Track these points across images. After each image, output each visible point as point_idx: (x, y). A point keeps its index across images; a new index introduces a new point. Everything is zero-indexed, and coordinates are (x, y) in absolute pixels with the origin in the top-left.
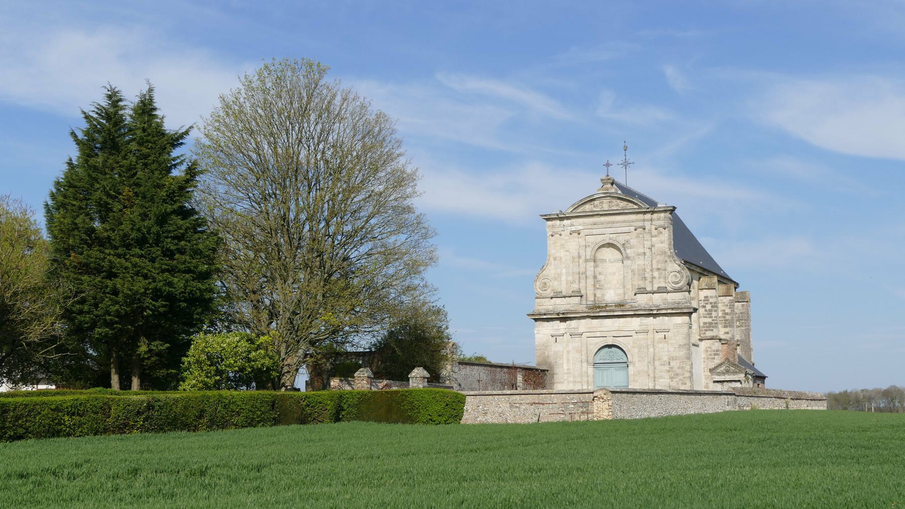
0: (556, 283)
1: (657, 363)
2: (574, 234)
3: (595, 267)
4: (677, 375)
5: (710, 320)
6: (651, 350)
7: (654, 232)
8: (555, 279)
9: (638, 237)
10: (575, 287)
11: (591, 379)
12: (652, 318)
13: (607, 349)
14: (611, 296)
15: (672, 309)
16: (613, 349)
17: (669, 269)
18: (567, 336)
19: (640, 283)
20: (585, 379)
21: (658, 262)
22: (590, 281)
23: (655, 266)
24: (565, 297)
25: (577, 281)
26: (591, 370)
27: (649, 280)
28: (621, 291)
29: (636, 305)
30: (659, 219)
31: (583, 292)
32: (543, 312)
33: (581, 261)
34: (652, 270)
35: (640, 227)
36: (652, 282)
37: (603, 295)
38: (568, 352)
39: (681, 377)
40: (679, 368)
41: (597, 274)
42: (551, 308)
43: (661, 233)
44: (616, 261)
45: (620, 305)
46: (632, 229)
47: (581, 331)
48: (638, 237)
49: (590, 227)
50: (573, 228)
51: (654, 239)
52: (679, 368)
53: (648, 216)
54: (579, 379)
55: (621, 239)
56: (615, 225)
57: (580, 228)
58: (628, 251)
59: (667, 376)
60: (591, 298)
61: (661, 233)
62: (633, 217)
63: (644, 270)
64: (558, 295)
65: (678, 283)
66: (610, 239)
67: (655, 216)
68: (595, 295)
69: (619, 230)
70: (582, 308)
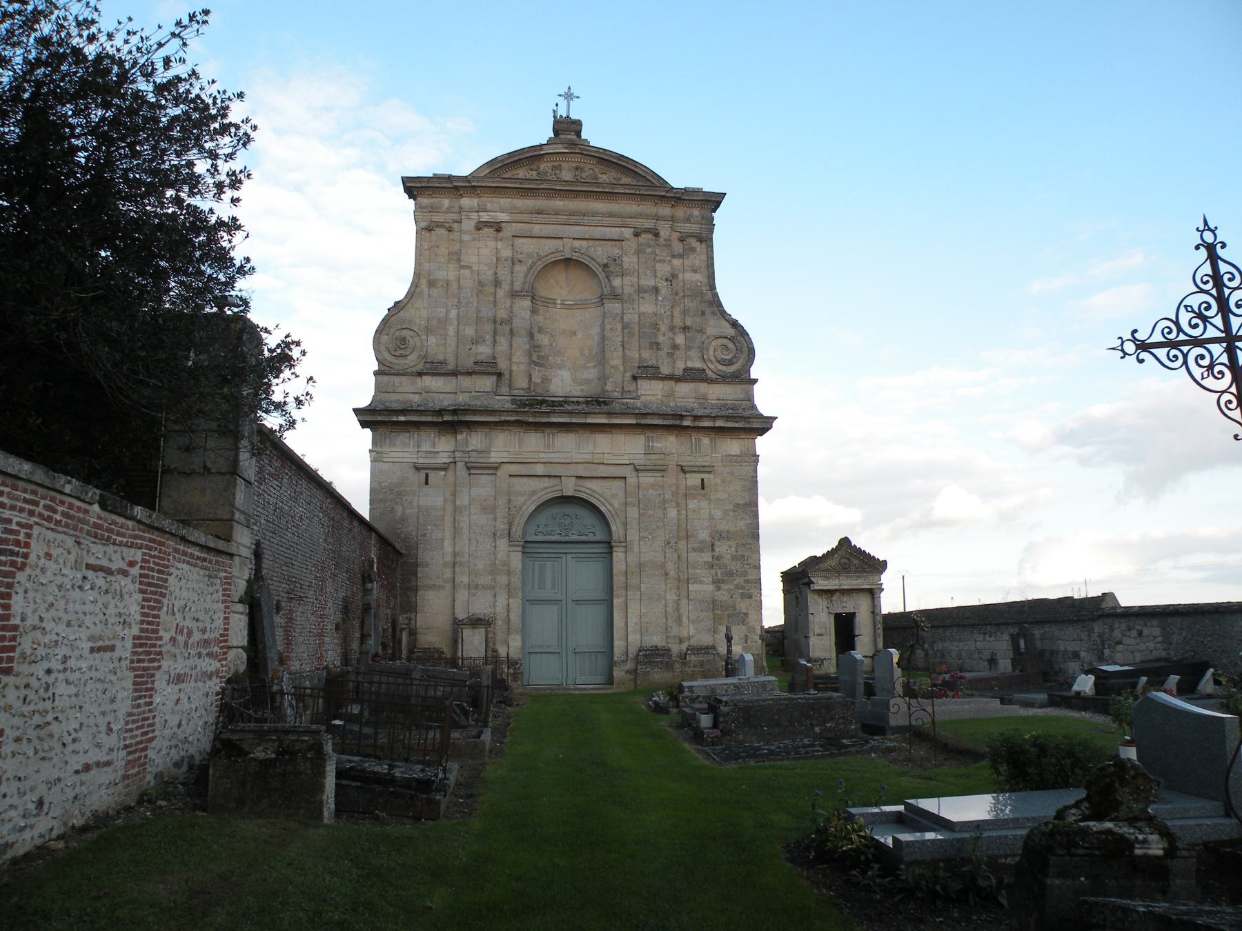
0: (432, 340)
2: (486, 231)
3: (534, 311)
4: (731, 574)
7: (678, 247)
8: (428, 330)
10: (484, 351)
11: (516, 580)
13: (556, 510)
14: (563, 382)
15: (728, 418)
17: (710, 331)
19: (646, 354)
20: (503, 579)
21: (684, 313)
22: (521, 343)
24: (455, 374)
26: (516, 559)
28: (592, 374)
30: (688, 220)
31: (502, 365)
32: (396, 406)
33: (500, 293)
34: (672, 328)
35: (648, 231)
37: (546, 380)
38: (457, 510)
39: (739, 580)
40: (734, 558)
41: (535, 330)
42: (416, 399)
43: (693, 250)
44: (581, 305)
45: (598, 402)
46: (628, 233)
47: (495, 457)
49: (526, 217)
50: (485, 217)
52: (734, 558)
53: (665, 210)
54: (486, 580)
55: (601, 253)
56: (586, 220)
57: (503, 217)
58: (617, 282)
59: (706, 575)
61: (693, 250)
62: (630, 207)
63: (655, 326)
64: (435, 369)
65: (730, 363)
66: (574, 250)
67: (680, 212)
69: (597, 232)
70: (502, 401)
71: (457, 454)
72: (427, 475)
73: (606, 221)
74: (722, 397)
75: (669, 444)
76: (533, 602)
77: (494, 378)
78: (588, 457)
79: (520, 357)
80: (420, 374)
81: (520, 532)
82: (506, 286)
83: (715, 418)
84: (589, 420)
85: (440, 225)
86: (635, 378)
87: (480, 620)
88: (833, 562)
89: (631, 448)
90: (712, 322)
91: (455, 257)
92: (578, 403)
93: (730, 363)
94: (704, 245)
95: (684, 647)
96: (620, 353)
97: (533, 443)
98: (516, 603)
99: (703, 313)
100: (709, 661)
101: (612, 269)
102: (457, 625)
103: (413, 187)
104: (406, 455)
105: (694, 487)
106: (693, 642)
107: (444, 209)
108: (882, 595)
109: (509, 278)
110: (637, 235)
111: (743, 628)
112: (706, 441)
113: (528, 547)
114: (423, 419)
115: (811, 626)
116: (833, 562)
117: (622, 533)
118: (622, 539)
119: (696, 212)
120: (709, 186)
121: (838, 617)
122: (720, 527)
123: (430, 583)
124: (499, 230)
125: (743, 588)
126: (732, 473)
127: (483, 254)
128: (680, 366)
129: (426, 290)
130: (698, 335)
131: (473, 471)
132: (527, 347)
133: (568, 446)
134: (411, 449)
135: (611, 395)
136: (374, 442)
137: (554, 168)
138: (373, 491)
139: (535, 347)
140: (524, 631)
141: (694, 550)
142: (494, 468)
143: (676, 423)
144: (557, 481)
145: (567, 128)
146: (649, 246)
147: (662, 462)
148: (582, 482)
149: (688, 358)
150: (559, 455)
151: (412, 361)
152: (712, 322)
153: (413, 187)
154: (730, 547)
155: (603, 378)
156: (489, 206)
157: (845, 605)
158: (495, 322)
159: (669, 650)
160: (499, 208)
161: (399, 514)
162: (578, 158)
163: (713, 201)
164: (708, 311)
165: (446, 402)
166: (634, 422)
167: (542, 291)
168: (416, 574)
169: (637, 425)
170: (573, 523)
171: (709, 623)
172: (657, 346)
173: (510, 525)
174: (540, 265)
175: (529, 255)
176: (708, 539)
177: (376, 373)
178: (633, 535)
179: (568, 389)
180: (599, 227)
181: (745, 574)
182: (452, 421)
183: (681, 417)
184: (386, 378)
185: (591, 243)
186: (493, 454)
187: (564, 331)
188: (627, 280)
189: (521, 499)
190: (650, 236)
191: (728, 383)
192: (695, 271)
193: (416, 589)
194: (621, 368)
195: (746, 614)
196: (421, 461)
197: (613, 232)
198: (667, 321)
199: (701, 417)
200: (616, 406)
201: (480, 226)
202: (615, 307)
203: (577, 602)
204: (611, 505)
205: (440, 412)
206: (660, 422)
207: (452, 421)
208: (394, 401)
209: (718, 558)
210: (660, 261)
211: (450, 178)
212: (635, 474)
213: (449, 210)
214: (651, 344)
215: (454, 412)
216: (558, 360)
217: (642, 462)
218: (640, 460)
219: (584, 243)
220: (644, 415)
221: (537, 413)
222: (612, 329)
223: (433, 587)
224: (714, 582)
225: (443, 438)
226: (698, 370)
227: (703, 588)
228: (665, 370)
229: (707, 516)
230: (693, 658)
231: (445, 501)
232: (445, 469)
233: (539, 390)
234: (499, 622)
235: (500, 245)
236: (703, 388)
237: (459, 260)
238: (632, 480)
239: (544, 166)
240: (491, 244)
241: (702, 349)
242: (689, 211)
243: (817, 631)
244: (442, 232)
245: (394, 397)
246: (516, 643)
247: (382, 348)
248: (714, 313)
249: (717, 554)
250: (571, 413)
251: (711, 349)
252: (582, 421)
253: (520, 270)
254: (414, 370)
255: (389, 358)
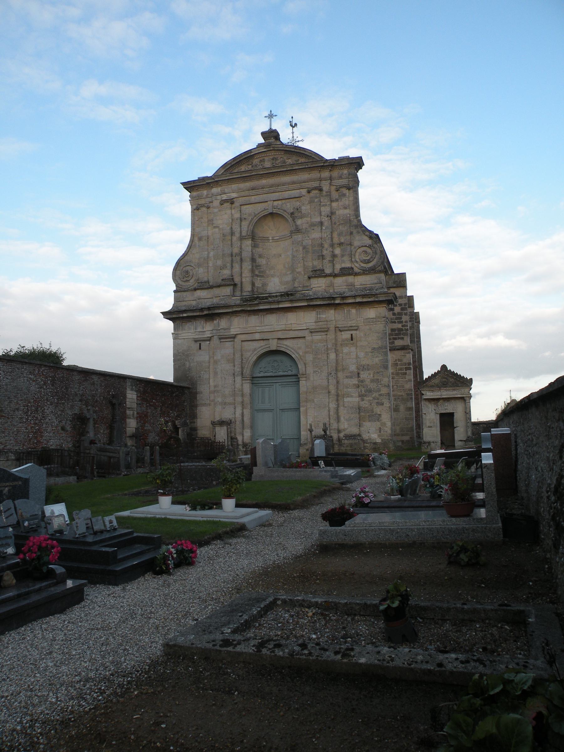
0: (201, 270)
1: (340, 374)
2: (227, 205)
3: (255, 246)
4: (370, 391)
5: (400, 326)
6: (333, 356)
7: (335, 195)
8: (199, 265)
9: (311, 202)
10: (226, 273)
11: (247, 399)
12: (332, 312)
14: (275, 285)
15: (363, 296)
16: (278, 358)
17: (356, 243)
18: (215, 340)
19: (316, 263)
20: (239, 399)
21: (340, 235)
22: (247, 266)
23: (336, 240)
24: (211, 287)
25: (229, 265)
26: (247, 387)
27: (328, 258)
28: (289, 278)
29: (311, 293)
30: (340, 177)
31: (237, 280)
32: (184, 308)
33: (235, 238)
34: (332, 245)
36: (332, 262)
37: (264, 285)
39: (375, 395)
41: (256, 256)
42: (194, 303)
43: (344, 195)
45: (287, 295)
46: (304, 192)
47: (233, 332)
48: (311, 202)
49: (247, 193)
50: (225, 197)
51: (334, 204)
52: (372, 381)
53: (326, 174)
54: (230, 400)
55: (289, 206)
57: (234, 195)
58: (299, 222)
59: (354, 392)
60: (248, 288)
61: (344, 195)
62: (305, 176)
63: (322, 245)
65: (369, 262)
66: (274, 207)
67: (335, 173)
68: (253, 284)
69: (287, 194)
71: (214, 332)
72: (200, 344)
73: (291, 187)
74: (363, 283)
75: (330, 315)
76: (258, 411)
77: (232, 287)
78: (283, 327)
79: (247, 274)
80: (195, 289)
81: (248, 372)
82: (237, 235)
83: (355, 297)
84: (281, 306)
85: (202, 206)
86: (309, 278)
87: (224, 421)
88: (436, 381)
89: (308, 319)
90: (357, 238)
91: (210, 222)
92: (276, 296)
93: (369, 262)
94: (351, 191)
95: (342, 435)
96: (302, 264)
97: (253, 321)
98: (247, 412)
99: (351, 233)
100: (355, 444)
101: (296, 215)
102: (214, 424)
103: (189, 186)
104: (190, 334)
105: (346, 340)
106: (348, 432)
107: (204, 196)
108: (472, 400)
109: (239, 229)
110: (309, 192)
111: (378, 423)
112: (354, 311)
113: (254, 380)
114: (195, 314)
115: (424, 422)
116: (436, 381)
117: (304, 369)
118: (304, 373)
119: (345, 172)
120: (353, 153)
121: (442, 415)
122: (364, 363)
123: (204, 402)
124: (232, 203)
125: (378, 399)
126: (370, 329)
127: (224, 218)
128: (338, 267)
129: (197, 243)
130: (349, 247)
131: (222, 340)
132: (250, 267)
133: (273, 322)
134: (192, 331)
135: (297, 289)
136: (175, 329)
137: (261, 161)
138: (175, 355)
139: (257, 266)
140: (252, 427)
141: (347, 377)
142: (234, 337)
143: (331, 302)
144: (265, 342)
145: (271, 136)
146: (316, 197)
147: (325, 326)
148: (280, 342)
149: (343, 262)
150: (267, 327)
151: (192, 283)
152: (357, 238)
153: (189, 186)
154: (370, 374)
155: (294, 280)
156: (226, 191)
157: (448, 408)
158: (232, 255)
159: (331, 437)
160: (231, 191)
161: (188, 366)
162: (273, 153)
163: (358, 163)
164: (355, 232)
165: (208, 303)
166: (306, 304)
167: (260, 233)
168: (196, 398)
169: (309, 306)
170: (275, 365)
171: (357, 421)
172: (323, 257)
173: (242, 368)
174: (256, 219)
175: (250, 215)
176: (356, 370)
177: (175, 292)
178: (310, 370)
179: (277, 288)
180: (286, 192)
181: (379, 390)
182: (210, 314)
183: (334, 298)
184: (179, 294)
185: (284, 201)
186: (232, 330)
187: (275, 255)
188: (304, 220)
189: (249, 354)
190: (317, 191)
191: (367, 274)
192: (345, 208)
193: (196, 406)
194: (303, 273)
195: (380, 415)
196: (197, 337)
197: (295, 193)
198: (329, 241)
199: (347, 297)
200: (298, 296)
201: (223, 202)
202: (299, 237)
203: (282, 410)
204: (298, 353)
205: (202, 310)
206: (319, 303)
207: (210, 314)
208: (183, 306)
209: (362, 381)
210: (323, 205)
211: (204, 179)
212: (310, 334)
213: (207, 197)
214: (319, 256)
215: (209, 308)
216: (272, 272)
217: (313, 327)
218: (313, 326)
219: (280, 202)
220: (311, 300)
221: (256, 304)
222: (297, 251)
223: (205, 405)
224: (359, 396)
225: (208, 324)
226: (349, 268)
227: (353, 400)
228: (328, 271)
229: (355, 356)
230: (346, 441)
231: (210, 358)
232: (209, 340)
233: (260, 291)
234: (238, 423)
235: (233, 211)
236: (350, 279)
237: (213, 224)
238: (309, 338)
239: (256, 161)
240: (229, 212)
241: (351, 255)
242: (341, 172)
243: (428, 424)
244: (204, 209)
245: (184, 303)
246: (247, 434)
247: (177, 278)
248: (358, 232)
249: (361, 379)
250: (270, 303)
251: (357, 254)
252: (276, 306)
253: (245, 224)
254: (192, 287)
255: (181, 283)
